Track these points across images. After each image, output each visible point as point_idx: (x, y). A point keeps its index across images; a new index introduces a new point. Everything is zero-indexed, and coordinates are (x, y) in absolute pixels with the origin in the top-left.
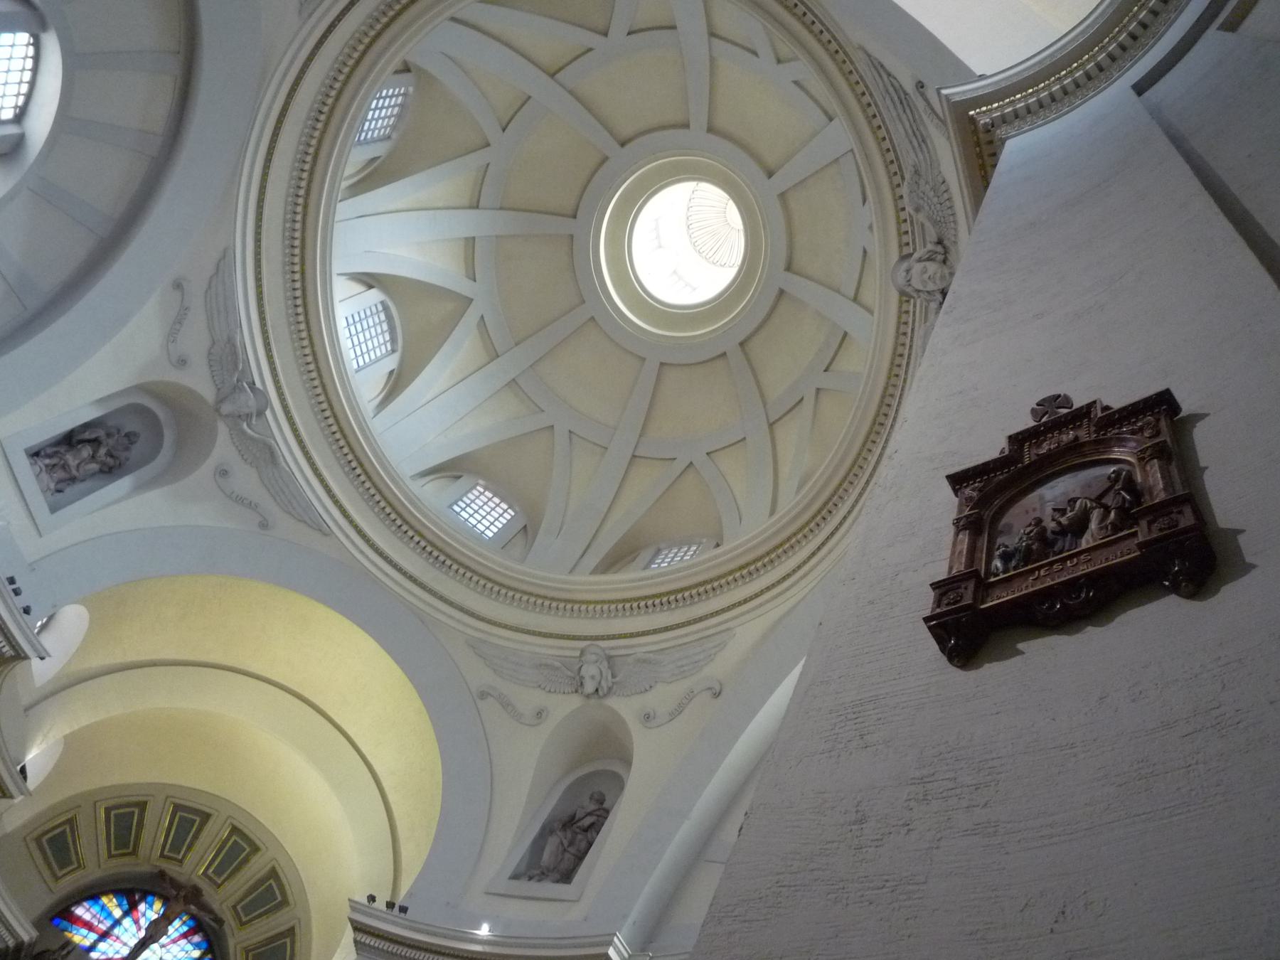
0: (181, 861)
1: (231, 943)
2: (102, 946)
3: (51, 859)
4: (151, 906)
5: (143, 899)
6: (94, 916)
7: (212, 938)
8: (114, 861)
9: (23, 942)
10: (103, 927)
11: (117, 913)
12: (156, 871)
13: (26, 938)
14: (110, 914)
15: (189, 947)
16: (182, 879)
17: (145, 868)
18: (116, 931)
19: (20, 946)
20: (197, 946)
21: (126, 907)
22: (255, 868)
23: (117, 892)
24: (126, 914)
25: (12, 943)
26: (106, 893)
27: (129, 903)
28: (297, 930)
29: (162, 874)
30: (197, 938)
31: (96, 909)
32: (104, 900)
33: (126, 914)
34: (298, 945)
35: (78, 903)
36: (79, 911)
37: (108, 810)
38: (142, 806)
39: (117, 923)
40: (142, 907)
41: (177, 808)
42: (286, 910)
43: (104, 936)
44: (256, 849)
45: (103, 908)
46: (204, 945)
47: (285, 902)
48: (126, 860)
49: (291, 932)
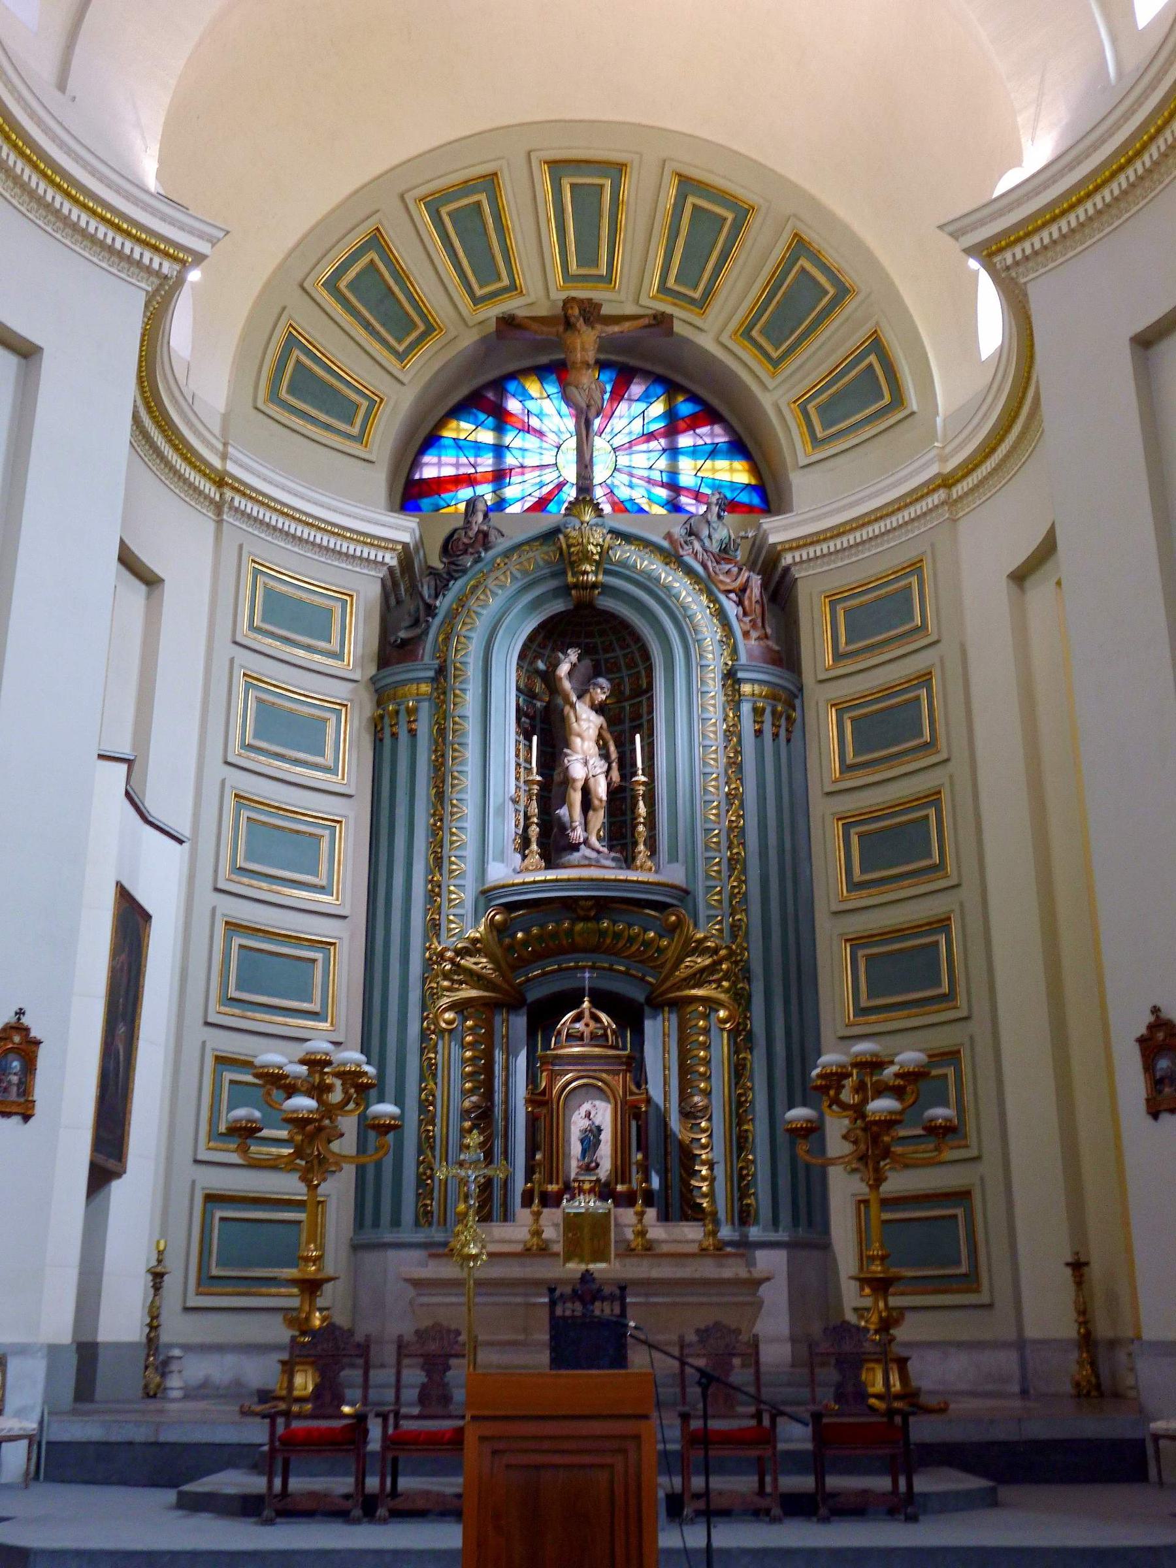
0: (513, 287)
1: (707, 342)
2: (509, 492)
3: (323, 417)
4: (525, 396)
5: (502, 393)
6: (457, 465)
7: (659, 370)
8: (416, 360)
9: (405, 546)
10: (486, 463)
11: (487, 436)
12: (492, 327)
13: (406, 537)
14: (478, 447)
15: (639, 407)
16: (542, 311)
17: (468, 339)
18: (510, 460)
19: (407, 556)
20: (646, 398)
21: (490, 421)
22: (645, 203)
23: (458, 411)
24: (499, 429)
25: (391, 559)
26: (442, 423)
27: (489, 413)
28: (809, 235)
29: (508, 323)
30: (636, 389)
31: (449, 456)
32: (448, 433)
33: (499, 429)
34: (832, 256)
35: (416, 464)
36: (428, 472)
37: (331, 285)
38: (376, 241)
39: (499, 450)
40: (513, 405)
41: (434, 203)
42: (755, 223)
43: (499, 476)
44: (617, 170)
45: (458, 444)
46: (659, 390)
47: (743, 212)
48: (429, 345)
49: (800, 246)
